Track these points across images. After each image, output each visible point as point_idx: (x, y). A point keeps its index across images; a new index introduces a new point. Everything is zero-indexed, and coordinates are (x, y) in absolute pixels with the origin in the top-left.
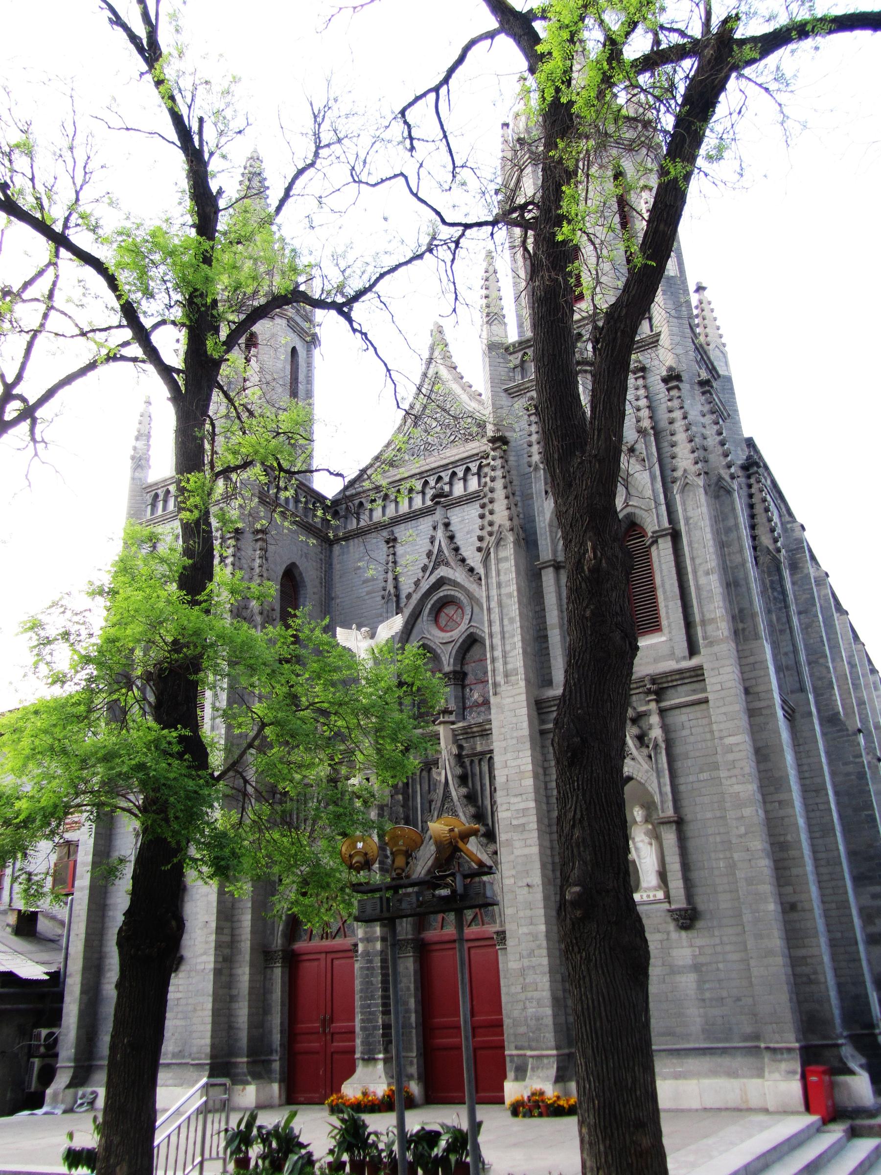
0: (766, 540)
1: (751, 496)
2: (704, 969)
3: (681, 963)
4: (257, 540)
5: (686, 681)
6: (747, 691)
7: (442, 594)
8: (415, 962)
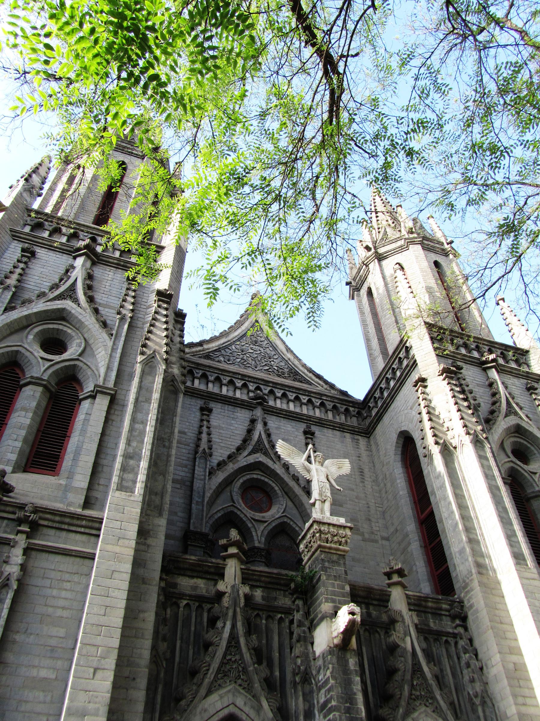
7: (255, 476)
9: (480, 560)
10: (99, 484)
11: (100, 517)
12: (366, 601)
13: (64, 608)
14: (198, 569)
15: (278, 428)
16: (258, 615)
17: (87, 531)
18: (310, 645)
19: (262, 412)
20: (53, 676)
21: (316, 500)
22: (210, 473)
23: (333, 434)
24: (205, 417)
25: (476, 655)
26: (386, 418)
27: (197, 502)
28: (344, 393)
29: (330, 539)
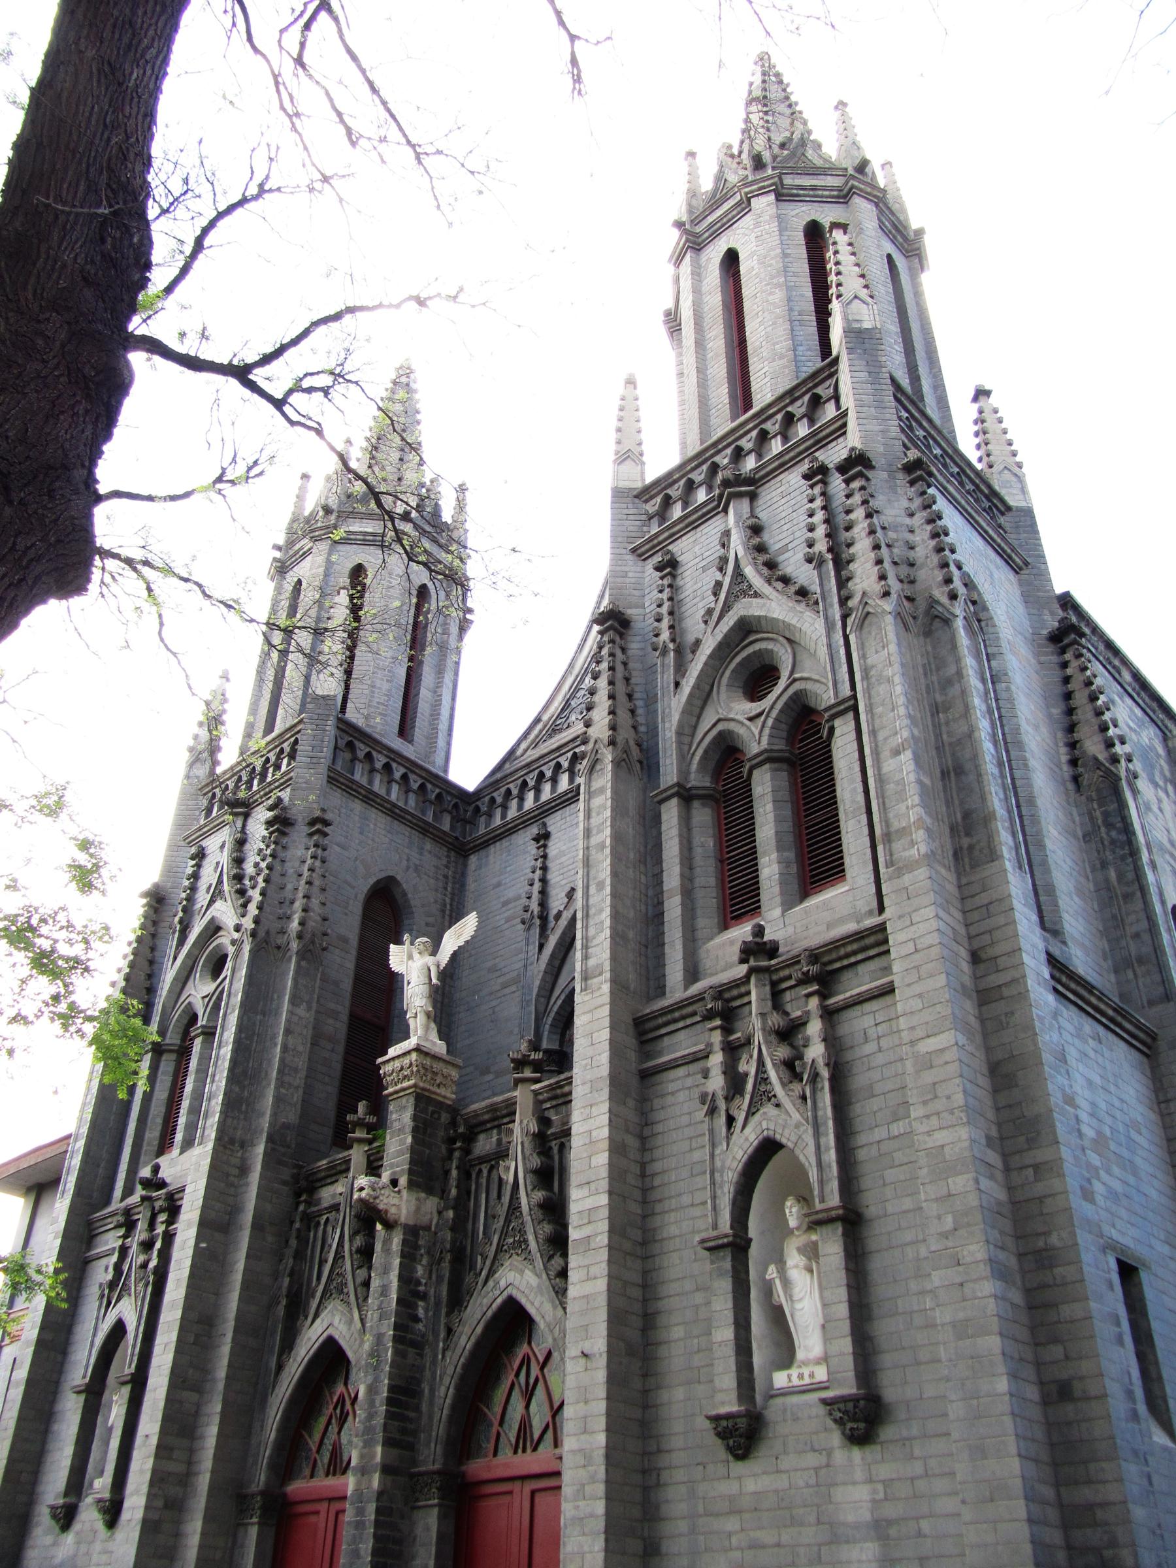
0: (1093, 747)
1: (1067, 680)
2: (893, 1532)
3: (851, 1518)
4: (311, 835)
5: (871, 953)
6: (976, 958)
8: (442, 1518)
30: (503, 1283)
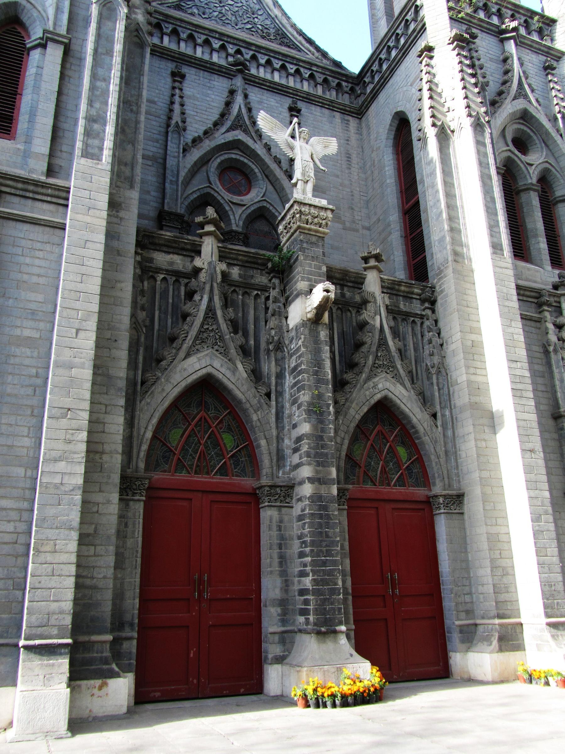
7: (234, 156)
9: (458, 249)
10: (61, 151)
11: (66, 186)
12: (341, 282)
13: (39, 275)
14: (174, 245)
15: (260, 102)
16: (234, 291)
17: (54, 200)
18: (284, 319)
19: (243, 82)
20: (38, 336)
21: (298, 180)
22: (184, 150)
23: (322, 113)
24: (177, 84)
25: (439, 334)
26: (382, 97)
27: (171, 181)
28: (338, 64)
29: (310, 221)
30: (380, 386)
